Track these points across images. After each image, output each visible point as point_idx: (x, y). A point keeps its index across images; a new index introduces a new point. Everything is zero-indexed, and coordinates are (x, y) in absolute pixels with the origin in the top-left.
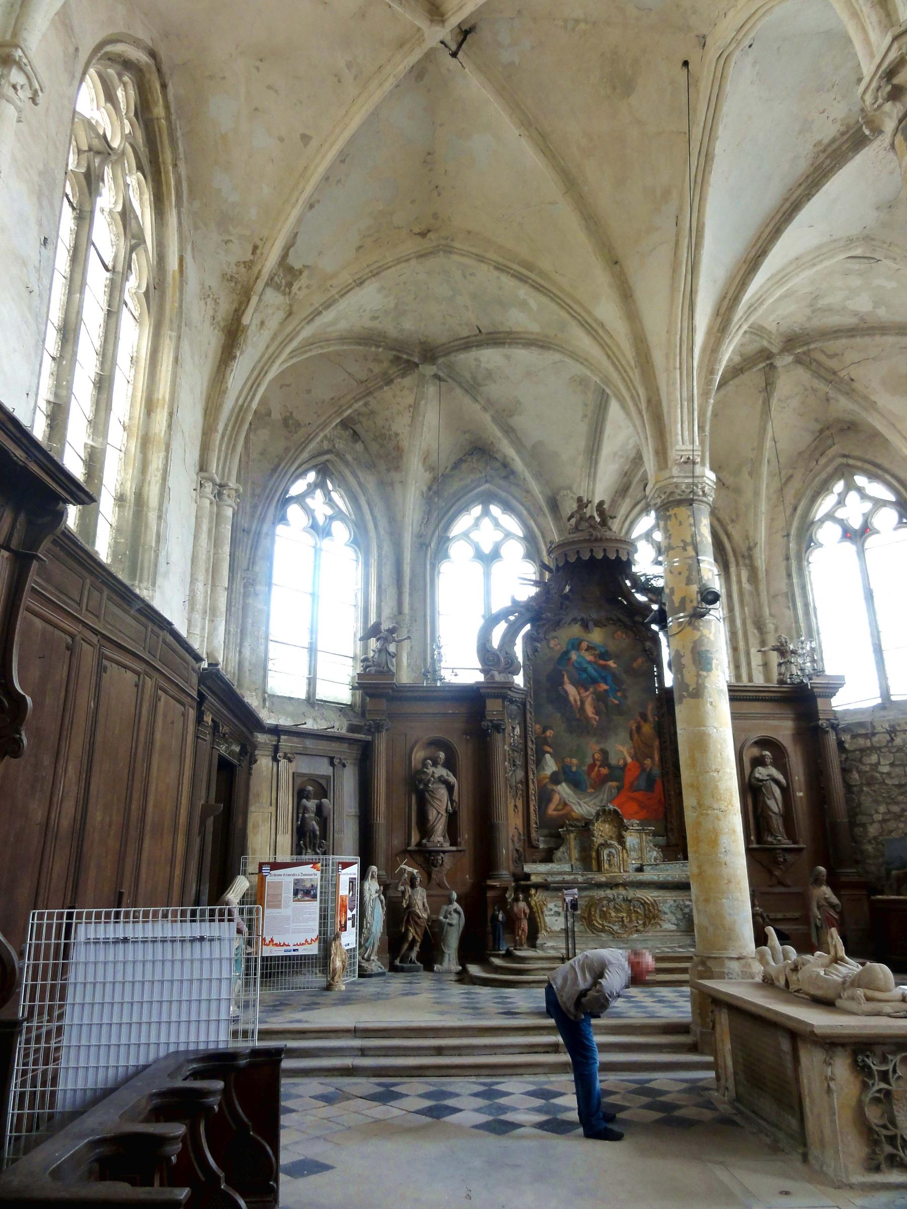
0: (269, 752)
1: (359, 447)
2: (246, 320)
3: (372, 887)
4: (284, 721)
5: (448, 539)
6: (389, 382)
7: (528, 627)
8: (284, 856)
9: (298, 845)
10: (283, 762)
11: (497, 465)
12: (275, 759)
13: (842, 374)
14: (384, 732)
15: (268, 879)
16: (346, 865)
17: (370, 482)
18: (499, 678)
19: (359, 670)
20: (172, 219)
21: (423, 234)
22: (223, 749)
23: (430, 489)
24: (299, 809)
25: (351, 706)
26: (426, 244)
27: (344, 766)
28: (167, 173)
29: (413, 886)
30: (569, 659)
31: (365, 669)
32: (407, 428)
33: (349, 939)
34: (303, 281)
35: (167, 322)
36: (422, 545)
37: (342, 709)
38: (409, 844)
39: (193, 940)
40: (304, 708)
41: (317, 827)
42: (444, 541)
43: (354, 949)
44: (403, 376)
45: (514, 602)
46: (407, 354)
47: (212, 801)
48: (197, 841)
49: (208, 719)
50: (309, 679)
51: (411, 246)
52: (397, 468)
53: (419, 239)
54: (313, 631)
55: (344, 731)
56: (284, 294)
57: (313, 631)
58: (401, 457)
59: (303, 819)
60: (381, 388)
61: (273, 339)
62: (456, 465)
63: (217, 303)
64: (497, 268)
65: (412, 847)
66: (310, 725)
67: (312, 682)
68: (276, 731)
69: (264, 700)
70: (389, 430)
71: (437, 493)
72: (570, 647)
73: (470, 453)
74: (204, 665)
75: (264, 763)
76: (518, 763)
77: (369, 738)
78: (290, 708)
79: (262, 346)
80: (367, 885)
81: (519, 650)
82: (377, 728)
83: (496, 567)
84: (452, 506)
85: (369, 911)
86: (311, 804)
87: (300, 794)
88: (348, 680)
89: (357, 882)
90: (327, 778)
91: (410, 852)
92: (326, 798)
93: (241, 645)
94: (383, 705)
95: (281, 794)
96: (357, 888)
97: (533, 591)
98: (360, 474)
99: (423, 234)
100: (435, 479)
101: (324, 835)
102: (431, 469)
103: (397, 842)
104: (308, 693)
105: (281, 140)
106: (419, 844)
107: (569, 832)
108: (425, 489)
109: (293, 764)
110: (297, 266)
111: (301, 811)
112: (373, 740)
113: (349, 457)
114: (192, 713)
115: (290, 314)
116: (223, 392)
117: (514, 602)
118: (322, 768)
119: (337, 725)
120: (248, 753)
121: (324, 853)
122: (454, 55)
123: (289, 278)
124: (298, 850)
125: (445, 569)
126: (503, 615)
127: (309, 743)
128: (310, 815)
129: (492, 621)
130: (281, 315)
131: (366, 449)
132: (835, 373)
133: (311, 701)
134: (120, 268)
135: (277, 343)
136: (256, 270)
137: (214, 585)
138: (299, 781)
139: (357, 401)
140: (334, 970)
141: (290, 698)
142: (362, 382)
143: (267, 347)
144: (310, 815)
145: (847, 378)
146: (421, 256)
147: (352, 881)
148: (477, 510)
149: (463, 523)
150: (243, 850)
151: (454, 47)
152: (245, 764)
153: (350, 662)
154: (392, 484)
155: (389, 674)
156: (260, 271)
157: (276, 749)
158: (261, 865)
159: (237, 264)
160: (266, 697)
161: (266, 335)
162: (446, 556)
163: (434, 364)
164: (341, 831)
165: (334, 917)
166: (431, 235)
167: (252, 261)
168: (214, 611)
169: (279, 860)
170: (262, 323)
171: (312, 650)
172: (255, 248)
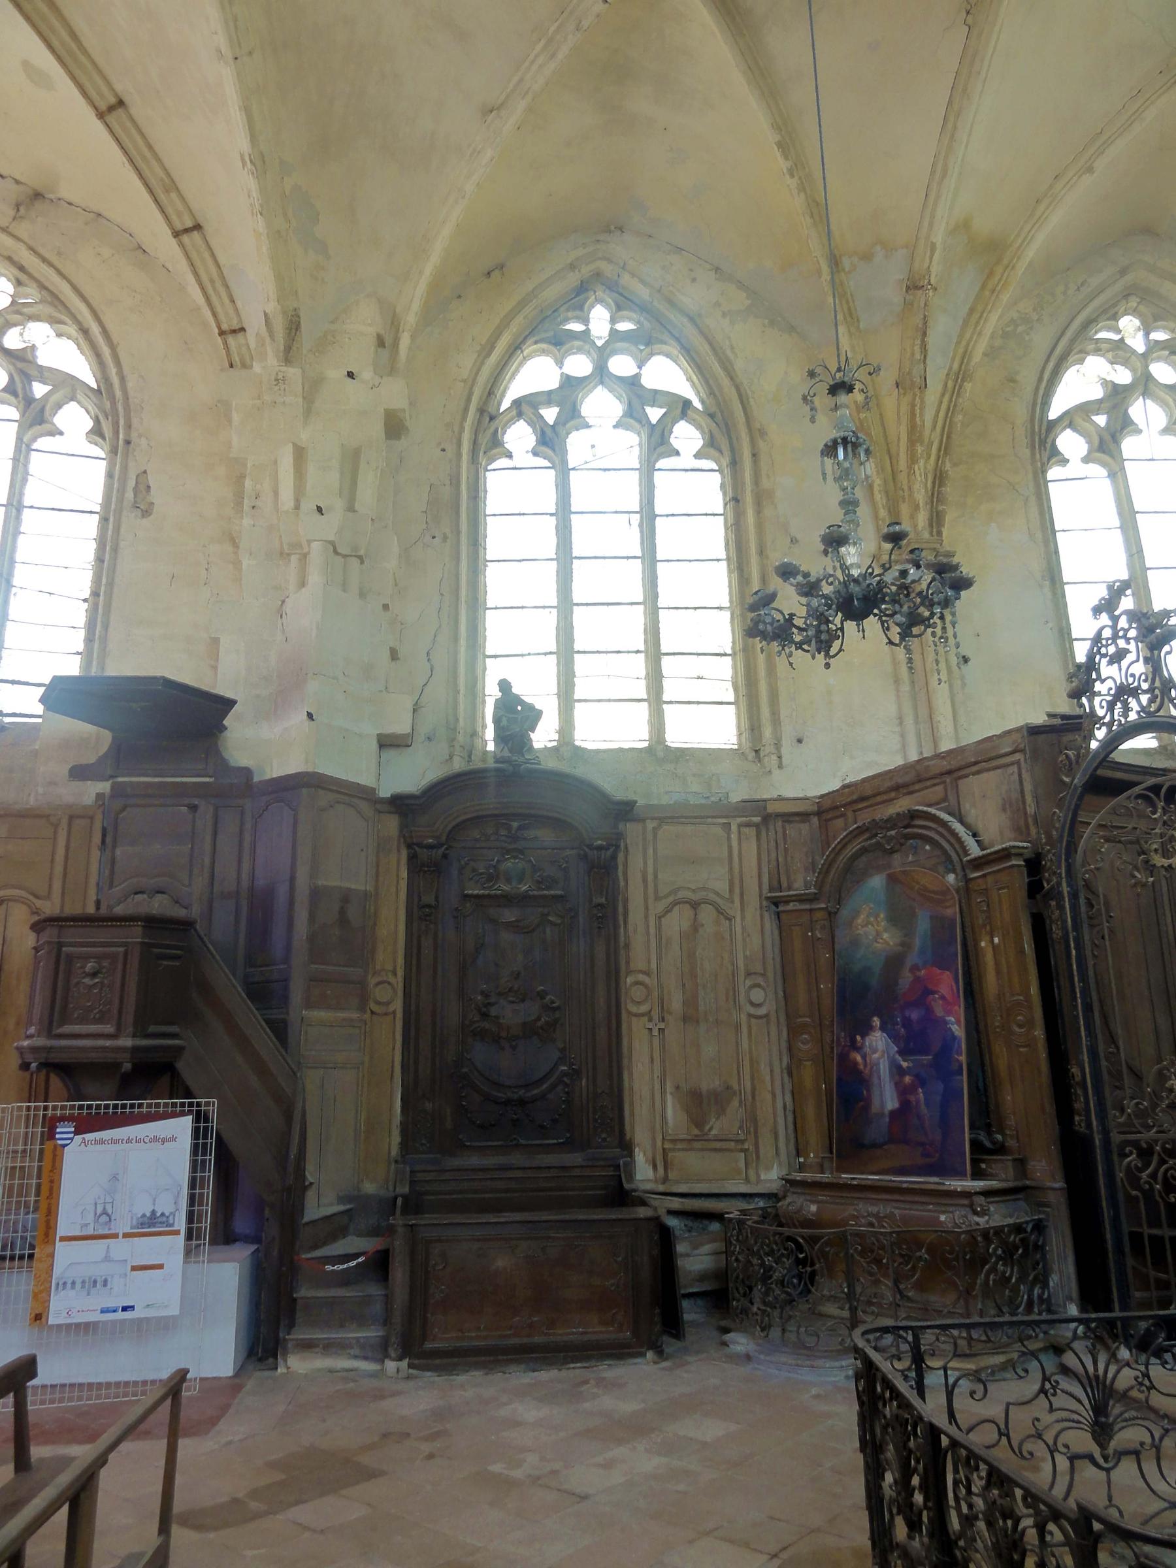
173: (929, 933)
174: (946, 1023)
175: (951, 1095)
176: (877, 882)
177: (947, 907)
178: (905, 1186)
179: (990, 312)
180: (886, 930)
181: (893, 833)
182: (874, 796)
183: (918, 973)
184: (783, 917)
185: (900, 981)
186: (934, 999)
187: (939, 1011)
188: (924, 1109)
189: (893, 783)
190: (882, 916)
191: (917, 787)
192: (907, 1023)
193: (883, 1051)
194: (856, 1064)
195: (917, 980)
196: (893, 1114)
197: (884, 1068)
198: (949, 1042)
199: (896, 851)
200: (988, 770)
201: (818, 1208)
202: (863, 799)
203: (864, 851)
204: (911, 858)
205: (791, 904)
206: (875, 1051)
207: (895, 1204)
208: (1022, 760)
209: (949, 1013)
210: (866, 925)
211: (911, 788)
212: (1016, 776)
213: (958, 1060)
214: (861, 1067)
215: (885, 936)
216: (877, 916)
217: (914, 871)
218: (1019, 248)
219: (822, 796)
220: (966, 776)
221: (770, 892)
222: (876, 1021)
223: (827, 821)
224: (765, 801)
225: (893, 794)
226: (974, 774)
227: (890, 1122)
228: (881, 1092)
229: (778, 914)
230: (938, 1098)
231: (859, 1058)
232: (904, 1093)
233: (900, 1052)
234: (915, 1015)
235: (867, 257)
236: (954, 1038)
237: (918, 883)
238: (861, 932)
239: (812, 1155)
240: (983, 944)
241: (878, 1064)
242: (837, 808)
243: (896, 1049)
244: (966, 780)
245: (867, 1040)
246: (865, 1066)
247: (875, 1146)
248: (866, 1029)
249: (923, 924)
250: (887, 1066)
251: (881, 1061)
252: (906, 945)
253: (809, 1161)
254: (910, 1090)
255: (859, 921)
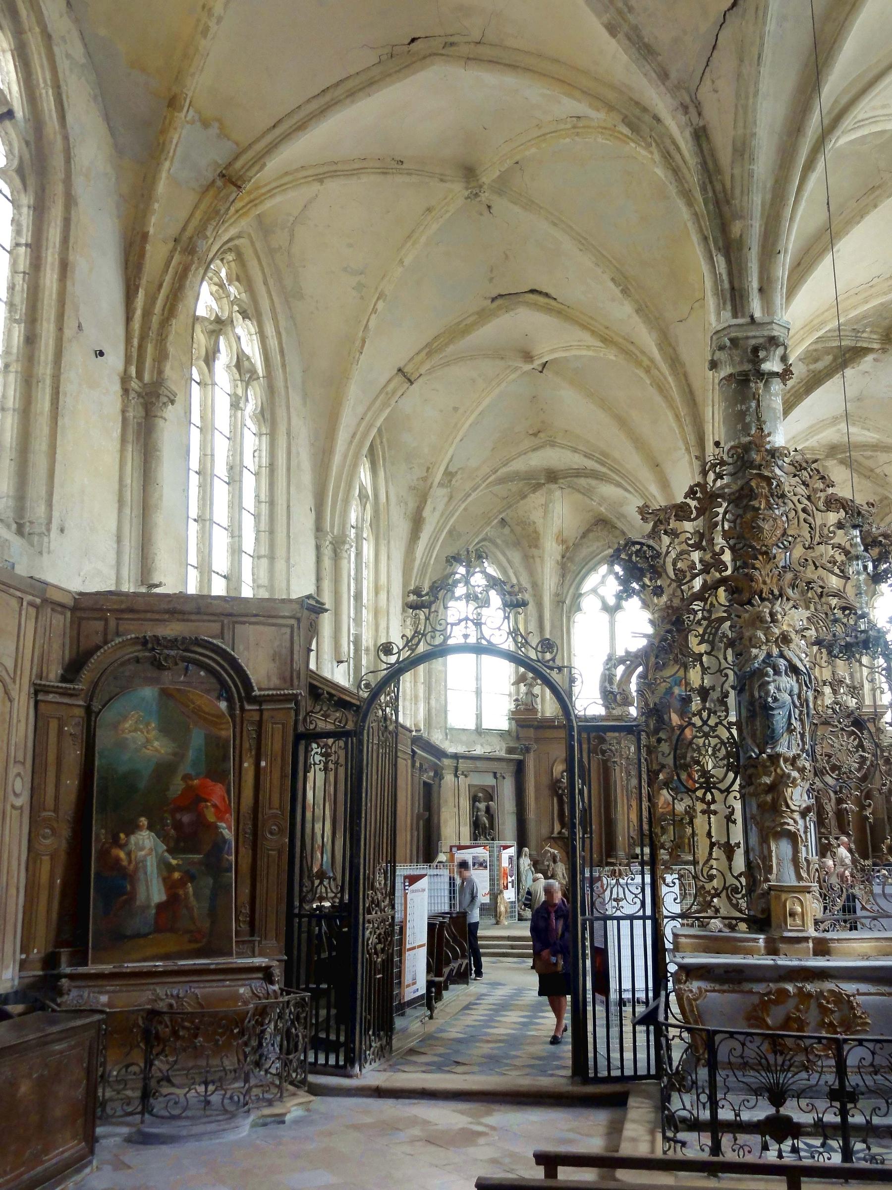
0: (452, 771)
1: (507, 530)
2: (426, 513)
3: (525, 862)
4: (460, 749)
5: (581, 595)
6: (524, 497)
7: (640, 669)
8: (465, 841)
9: (474, 833)
10: (461, 778)
11: (618, 533)
12: (456, 776)
13: (878, 471)
14: (532, 754)
15: (456, 856)
16: (506, 847)
17: (516, 556)
18: (617, 712)
19: (512, 707)
20: (381, 474)
21: (535, 435)
22: (425, 778)
23: (563, 557)
24: (474, 808)
25: (509, 732)
26: (537, 441)
27: (504, 778)
28: (377, 449)
29: (555, 862)
30: (673, 693)
31: (517, 706)
32: (542, 520)
33: (510, 895)
34: (459, 476)
35: (381, 535)
36: (559, 601)
37: (502, 734)
38: (552, 832)
39: (434, 875)
40: (474, 737)
41: (486, 822)
42: (578, 596)
43: (515, 902)
44: (534, 491)
45: (627, 652)
46: (535, 479)
47: (421, 810)
48: (416, 833)
49: (418, 764)
50: (477, 715)
51: (527, 443)
52: (536, 547)
53: (533, 437)
54: (478, 679)
55: (503, 754)
56: (447, 487)
57: (478, 679)
58: (538, 539)
59: (477, 816)
60: (518, 502)
61: (441, 516)
62: (584, 535)
63: (406, 504)
64: (585, 456)
65: (555, 835)
66: (479, 751)
67: (479, 717)
68: (456, 757)
69: (446, 735)
70: (529, 518)
71: (571, 559)
72: (673, 684)
73: (596, 524)
74: (414, 733)
75: (449, 778)
76: (633, 773)
77: (521, 757)
78: (464, 738)
79: (434, 525)
80: (521, 861)
81: (633, 687)
82: (527, 750)
83: (619, 615)
84: (583, 568)
85: (523, 878)
86: (482, 806)
87: (475, 799)
88: (506, 712)
89: (515, 858)
90: (493, 787)
91: (553, 838)
92: (492, 801)
93: (429, 699)
94: (531, 732)
95: (461, 799)
96: (515, 862)
97: (643, 643)
98: (508, 553)
99: (535, 435)
100: (567, 548)
101: (492, 827)
102: (563, 542)
103: (545, 831)
104: (477, 725)
105: (441, 411)
106: (560, 833)
107: (669, 824)
108: (559, 558)
109: (468, 778)
110: (454, 470)
111: (475, 810)
112: (524, 758)
113: (499, 541)
114: (409, 762)
115: (451, 498)
116: (414, 560)
117: (627, 652)
118: (489, 781)
119: (498, 748)
120: (438, 775)
121: (493, 839)
122: (541, 372)
123: (449, 478)
124: (475, 837)
125: (578, 617)
126: (622, 661)
127: (479, 764)
128: (482, 813)
129: (612, 662)
130: (446, 499)
131: (512, 531)
132: (872, 470)
133: (479, 731)
134: (360, 525)
135: (444, 517)
136: (429, 482)
137: (415, 682)
138: (473, 790)
139: (500, 512)
140: (500, 912)
141: (464, 730)
142: (504, 499)
143: (438, 522)
144: (482, 813)
145: (882, 474)
146: (535, 449)
147: (510, 858)
148: (604, 569)
149: (591, 581)
150: (439, 839)
151: (540, 369)
152: (437, 780)
153: (507, 698)
154: (533, 557)
155: (534, 710)
156: (432, 484)
157: (456, 769)
158: (451, 847)
159: (418, 479)
160: (449, 732)
161: (437, 514)
162: (579, 609)
163: (556, 483)
164: (503, 824)
165: (498, 880)
166: (541, 435)
167: (426, 477)
168: (416, 697)
169: (462, 844)
170: (434, 509)
171: (478, 693)
172: (428, 469)
173: (203, 748)
174: (217, 827)
175: (220, 890)
176: (149, 693)
177: (222, 729)
178: (213, 967)
179: (231, 225)
180: (157, 739)
181: (173, 653)
182: (146, 612)
183: (190, 782)
184: (42, 706)
185: (172, 788)
186: (207, 807)
187: (211, 818)
188: (192, 900)
189: (171, 606)
190: (153, 725)
191: (193, 617)
192: (178, 826)
193: (151, 850)
194: (118, 860)
195: (189, 789)
196: (160, 907)
197: (151, 865)
198: (219, 844)
199: (169, 669)
200: (264, 624)
201: (109, 998)
202: (131, 610)
203: (138, 660)
204: (182, 678)
205: (51, 696)
206: (142, 849)
207: (195, 985)
208: (296, 626)
209: (221, 819)
210: (135, 730)
211: (186, 617)
212: (288, 636)
213: (227, 860)
214: (125, 863)
215: (156, 744)
216: (148, 724)
217: (189, 691)
218: (264, 194)
219: (81, 594)
220: (244, 623)
221: (61, 682)
222: (144, 821)
223: (81, 619)
224: (47, 584)
225: (167, 616)
226: (251, 623)
227: (157, 914)
228: (147, 887)
229: (37, 703)
230: (207, 892)
231: (122, 855)
232: (171, 887)
233: (169, 851)
234: (186, 818)
235: (206, 124)
236: (225, 841)
237: (194, 703)
238: (128, 736)
239: (35, 951)
240: (246, 765)
241: (144, 861)
242: (101, 610)
243: (165, 848)
244: (242, 626)
245: (133, 839)
246: (130, 862)
247: (138, 936)
248: (132, 828)
249: (197, 738)
250: (155, 864)
251: (149, 858)
252: (179, 756)
253: (31, 956)
254: (182, 883)
255: (127, 725)
